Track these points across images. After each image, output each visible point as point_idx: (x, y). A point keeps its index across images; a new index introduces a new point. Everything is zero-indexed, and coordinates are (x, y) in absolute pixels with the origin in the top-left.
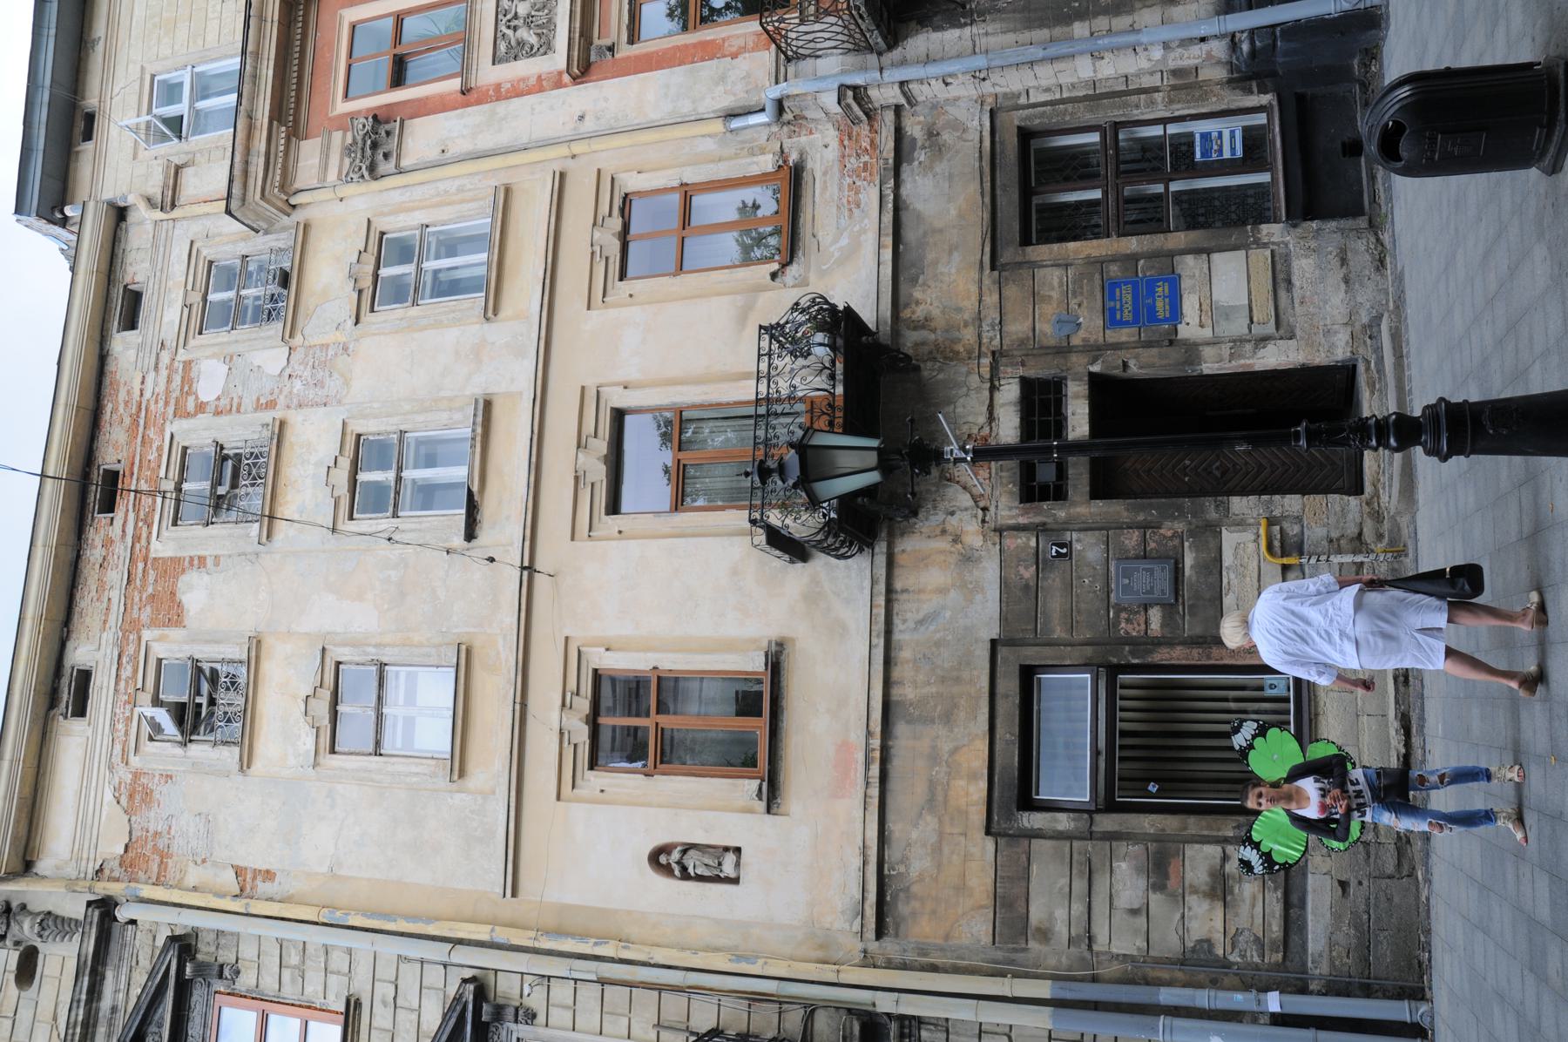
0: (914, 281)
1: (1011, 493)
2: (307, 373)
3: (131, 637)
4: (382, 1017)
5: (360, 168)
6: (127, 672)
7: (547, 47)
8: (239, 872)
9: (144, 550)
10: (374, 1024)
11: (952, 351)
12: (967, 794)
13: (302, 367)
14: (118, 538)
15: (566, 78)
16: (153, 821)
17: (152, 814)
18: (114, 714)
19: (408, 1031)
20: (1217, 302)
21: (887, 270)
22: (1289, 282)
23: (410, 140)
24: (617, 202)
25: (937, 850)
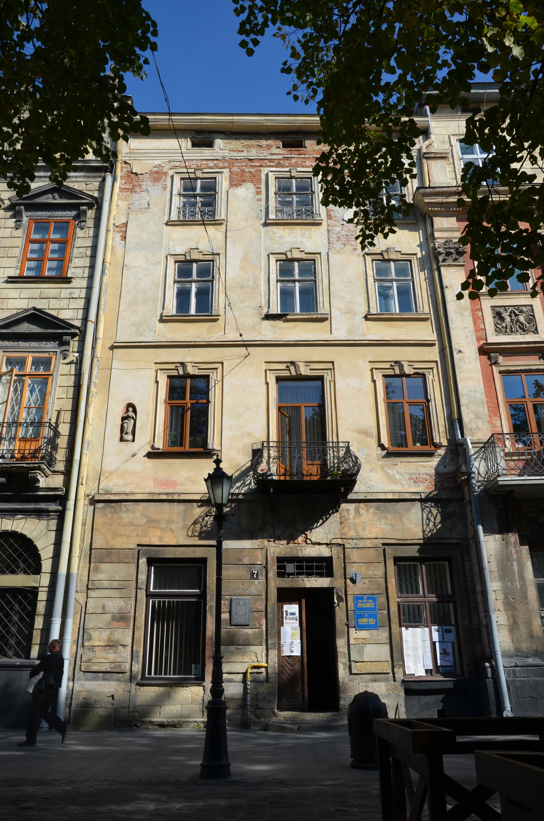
0: (378, 509)
1: (281, 553)
2: (344, 233)
3: (226, 164)
4: (65, 293)
5: (439, 248)
6: (211, 164)
7: (498, 331)
8: (126, 225)
9: (265, 165)
10: (63, 290)
11: (345, 526)
12: (154, 536)
13: (347, 230)
14: (270, 152)
15: (482, 342)
16: (146, 183)
17: (149, 183)
18: (192, 160)
19: (59, 304)
20: (366, 647)
21: (382, 497)
22: (375, 681)
23: (453, 270)
24: (421, 371)
25: (131, 524)
